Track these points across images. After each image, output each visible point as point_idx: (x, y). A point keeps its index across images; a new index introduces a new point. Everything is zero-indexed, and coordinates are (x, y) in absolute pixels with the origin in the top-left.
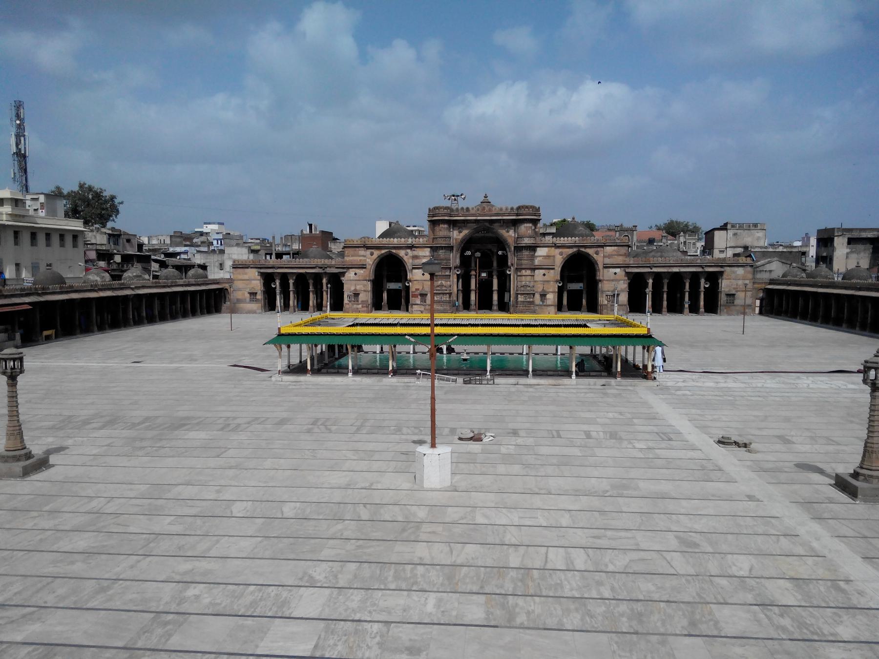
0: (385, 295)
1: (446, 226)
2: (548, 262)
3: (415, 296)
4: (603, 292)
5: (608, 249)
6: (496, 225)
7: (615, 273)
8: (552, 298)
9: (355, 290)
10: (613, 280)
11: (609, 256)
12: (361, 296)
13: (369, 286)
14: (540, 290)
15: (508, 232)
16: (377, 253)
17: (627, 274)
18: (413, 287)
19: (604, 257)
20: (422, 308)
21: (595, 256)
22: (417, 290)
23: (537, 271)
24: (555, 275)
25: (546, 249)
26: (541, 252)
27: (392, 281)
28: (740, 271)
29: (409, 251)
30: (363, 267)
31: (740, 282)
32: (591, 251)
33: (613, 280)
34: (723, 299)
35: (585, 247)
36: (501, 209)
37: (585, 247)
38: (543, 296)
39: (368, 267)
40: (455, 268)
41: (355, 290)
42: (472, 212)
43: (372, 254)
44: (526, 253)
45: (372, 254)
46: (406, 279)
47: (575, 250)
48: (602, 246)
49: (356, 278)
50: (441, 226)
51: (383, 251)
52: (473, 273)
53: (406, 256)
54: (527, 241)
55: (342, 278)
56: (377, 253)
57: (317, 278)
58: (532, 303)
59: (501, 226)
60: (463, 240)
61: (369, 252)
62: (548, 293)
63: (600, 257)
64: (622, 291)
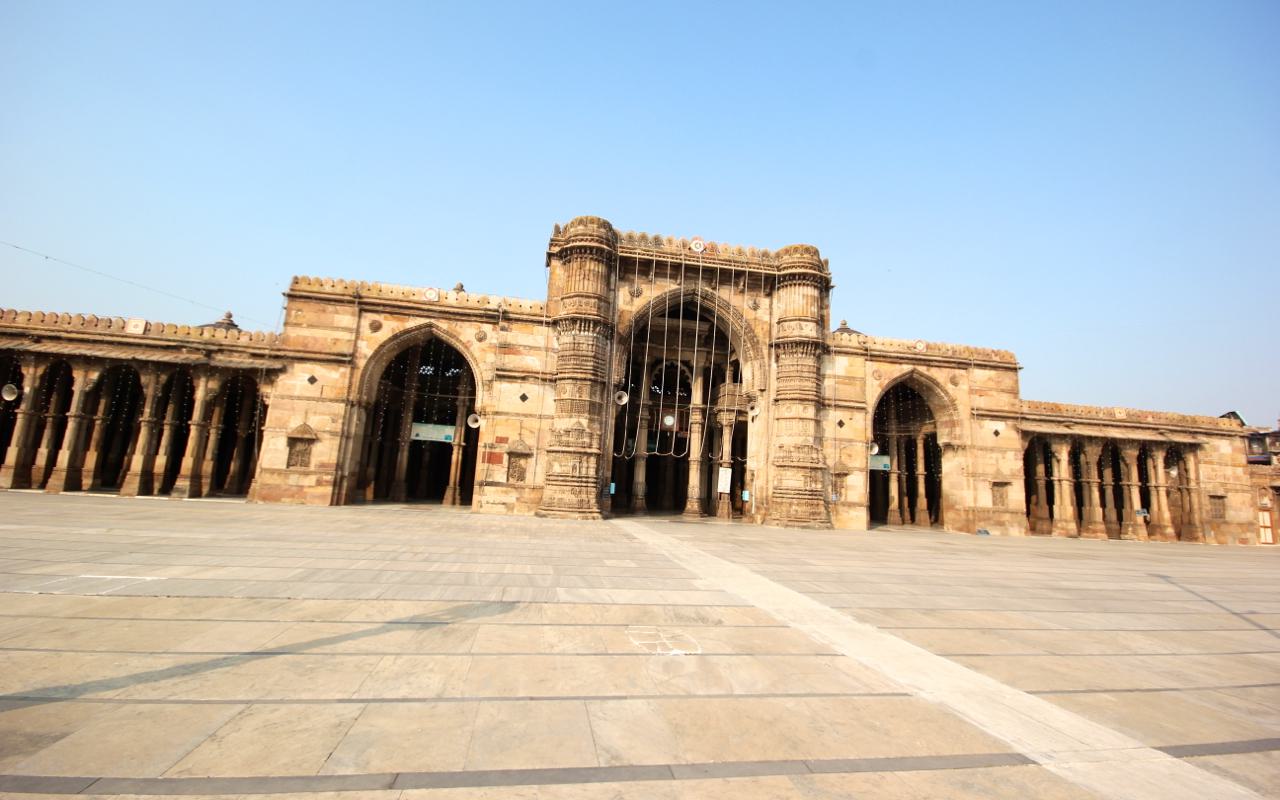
0: (404, 457)
1: (602, 268)
2: (848, 393)
3: (493, 459)
5: (978, 373)
6: (725, 293)
7: (997, 433)
8: (857, 487)
9: (305, 428)
10: (992, 450)
11: (980, 392)
12: (317, 448)
15: (756, 307)
16: (391, 326)
17: (1025, 434)
18: (488, 432)
19: (972, 391)
20: (512, 497)
21: (950, 387)
22: (502, 440)
24: (860, 425)
26: (838, 366)
27: (428, 421)
28: (1224, 447)
29: (487, 328)
30: (338, 360)
31: (1229, 471)
32: (940, 375)
33: (992, 450)
34: (1201, 507)
35: (927, 363)
36: (740, 253)
37: (927, 363)
39: (362, 363)
41: (305, 428)
42: (666, 248)
45: (376, 327)
46: (471, 410)
47: (907, 368)
48: (964, 365)
49: (313, 391)
50: (591, 266)
51: (413, 323)
53: (477, 345)
55: (265, 389)
57: (179, 379)
61: (369, 318)
63: (961, 392)
64: (1013, 475)
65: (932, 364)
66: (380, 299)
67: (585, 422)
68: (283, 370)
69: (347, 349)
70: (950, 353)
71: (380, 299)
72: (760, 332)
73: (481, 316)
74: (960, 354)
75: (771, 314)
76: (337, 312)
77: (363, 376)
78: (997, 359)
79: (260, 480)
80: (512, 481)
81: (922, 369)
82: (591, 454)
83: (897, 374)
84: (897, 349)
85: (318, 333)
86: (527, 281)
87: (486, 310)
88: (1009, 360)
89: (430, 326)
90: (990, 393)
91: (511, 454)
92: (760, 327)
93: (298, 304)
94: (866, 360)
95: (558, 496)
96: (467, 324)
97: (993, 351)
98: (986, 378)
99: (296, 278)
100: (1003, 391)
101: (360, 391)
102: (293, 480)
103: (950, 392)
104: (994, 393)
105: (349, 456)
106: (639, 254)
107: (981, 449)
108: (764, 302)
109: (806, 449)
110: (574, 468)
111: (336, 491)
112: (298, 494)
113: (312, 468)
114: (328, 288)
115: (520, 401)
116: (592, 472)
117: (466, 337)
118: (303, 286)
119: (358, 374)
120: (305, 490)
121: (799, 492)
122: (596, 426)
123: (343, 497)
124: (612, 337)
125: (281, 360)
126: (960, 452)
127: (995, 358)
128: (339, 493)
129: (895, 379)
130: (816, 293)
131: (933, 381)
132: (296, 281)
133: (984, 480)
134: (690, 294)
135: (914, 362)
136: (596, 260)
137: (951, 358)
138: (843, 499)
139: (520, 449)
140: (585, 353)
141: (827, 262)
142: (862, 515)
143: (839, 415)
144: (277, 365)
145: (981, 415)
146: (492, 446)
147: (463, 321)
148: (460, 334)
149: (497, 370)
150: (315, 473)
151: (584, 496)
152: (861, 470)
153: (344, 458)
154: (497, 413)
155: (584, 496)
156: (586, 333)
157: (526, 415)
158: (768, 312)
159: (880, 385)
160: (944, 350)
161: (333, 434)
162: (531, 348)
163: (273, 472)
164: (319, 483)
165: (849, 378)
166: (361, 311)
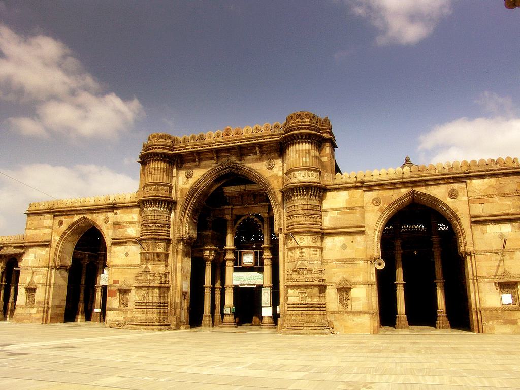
1: (161, 165)
2: (351, 220)
4: (477, 279)
5: (476, 182)
11: (483, 199)
12: (38, 292)
13: (61, 279)
14: (336, 279)
15: (270, 168)
16: (68, 221)
19: (470, 201)
21: (449, 201)
22: (116, 282)
23: (328, 241)
25: (344, 195)
26: (334, 201)
29: (110, 215)
30: (46, 245)
32: (439, 192)
38: (344, 290)
39: (54, 245)
40: (181, 240)
42: (208, 140)
43: (61, 224)
44: (300, 201)
45: (61, 224)
51: (76, 218)
52: (230, 256)
54: (301, 177)
56: (68, 221)
58: (321, 307)
59: (257, 160)
60: (192, 192)
62: (356, 284)
65: (427, 183)
66: (62, 208)
67: (150, 266)
68: (23, 254)
69: (48, 238)
70: (446, 171)
71: (62, 208)
72: (276, 186)
73: (105, 208)
74: (456, 170)
75: (283, 169)
76: (44, 219)
77: (56, 252)
78: (498, 166)
79: (18, 311)
80: (122, 307)
81: (421, 190)
82: (154, 287)
83: (395, 197)
84: (394, 176)
85: (38, 231)
86: (123, 183)
87: (108, 204)
88: (512, 165)
89: (85, 218)
90: (490, 199)
91: (120, 291)
92: (275, 182)
93: (32, 217)
94: (364, 191)
95: (136, 315)
96: (100, 214)
97: (493, 160)
98: (485, 187)
99: (30, 204)
100: (506, 195)
101: (55, 260)
102: (28, 309)
103: (450, 205)
104: (497, 199)
105: (51, 296)
106: (190, 149)
107: (486, 253)
108: (278, 162)
109: (301, 271)
110: (144, 297)
111: (45, 316)
112: (29, 318)
113: (35, 304)
114: (42, 207)
115: (126, 257)
116: (156, 299)
117: (99, 219)
118: (33, 208)
119: (53, 251)
120: (33, 316)
121: (298, 305)
122: (162, 269)
123: (49, 319)
124: (175, 208)
125: (25, 247)
126: (468, 258)
127: (496, 167)
128: (47, 318)
129: (393, 203)
130: (307, 146)
131: (435, 200)
132: (31, 205)
133: (489, 282)
134: (227, 168)
135: (412, 185)
136: (156, 161)
137: (447, 174)
138: (349, 307)
139: (124, 287)
140: (150, 221)
141: (327, 120)
142: (369, 322)
143: (339, 240)
144: (21, 251)
145: (477, 222)
146: (111, 286)
147: (98, 213)
148: (97, 220)
149: (113, 239)
150: (35, 306)
151: (150, 315)
152: (364, 283)
153: (48, 298)
154: (113, 266)
155: (150, 315)
156: (151, 209)
157: (127, 266)
158: (281, 169)
159: (380, 210)
160: (440, 169)
161: (43, 284)
162: (131, 223)
163: (21, 307)
164: (38, 312)
165: (349, 208)
166: (55, 216)
